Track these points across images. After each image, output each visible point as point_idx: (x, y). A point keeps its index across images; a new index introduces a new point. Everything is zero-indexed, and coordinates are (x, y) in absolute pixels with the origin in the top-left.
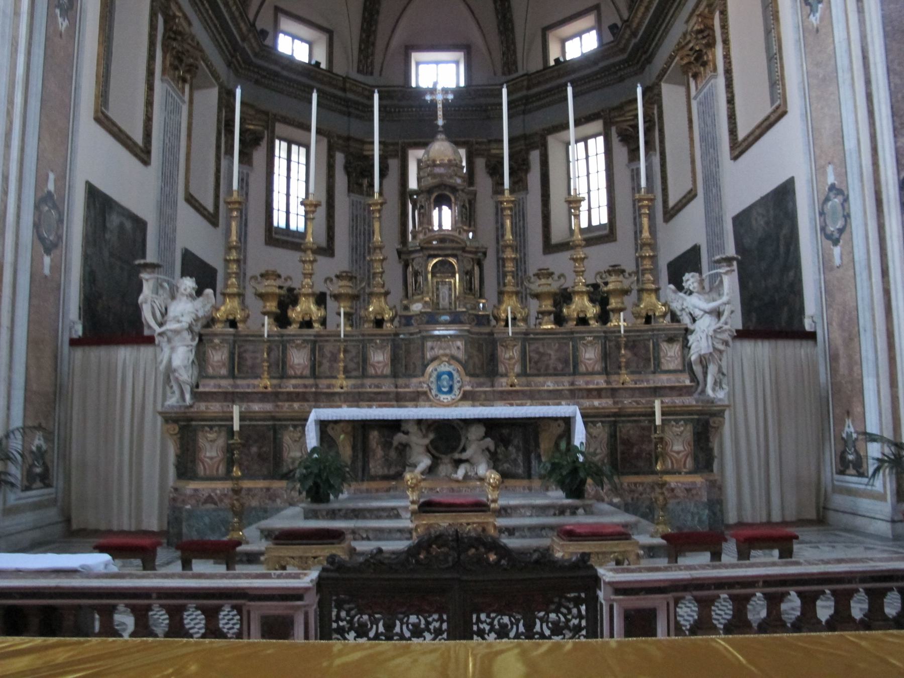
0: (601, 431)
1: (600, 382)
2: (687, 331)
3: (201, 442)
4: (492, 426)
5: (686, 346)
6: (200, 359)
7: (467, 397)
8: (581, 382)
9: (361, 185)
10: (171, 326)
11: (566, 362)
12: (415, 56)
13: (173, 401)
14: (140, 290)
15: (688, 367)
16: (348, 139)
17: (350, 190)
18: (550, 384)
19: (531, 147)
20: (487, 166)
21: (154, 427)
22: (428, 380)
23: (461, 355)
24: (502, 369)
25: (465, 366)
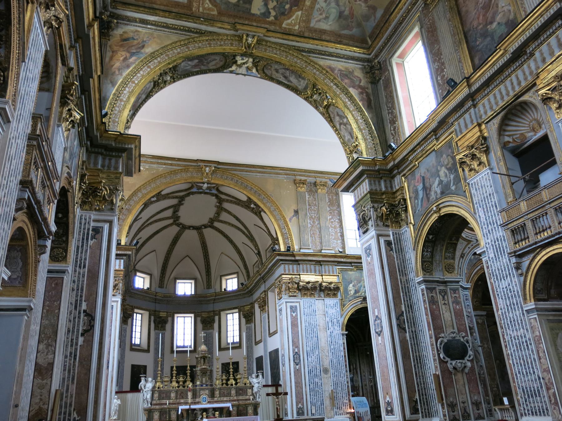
0: (235, 408)
1: (235, 398)
2: (253, 386)
3: (154, 415)
5: (252, 390)
7: (209, 402)
8: (231, 398)
9: (158, 327)
10: (147, 389)
11: (228, 394)
13: (146, 406)
14: (140, 381)
15: (253, 394)
16: (155, 311)
17: (155, 329)
18: (225, 399)
19: (215, 315)
20: (201, 320)
23: (207, 393)
24: (215, 396)
25: (208, 395)
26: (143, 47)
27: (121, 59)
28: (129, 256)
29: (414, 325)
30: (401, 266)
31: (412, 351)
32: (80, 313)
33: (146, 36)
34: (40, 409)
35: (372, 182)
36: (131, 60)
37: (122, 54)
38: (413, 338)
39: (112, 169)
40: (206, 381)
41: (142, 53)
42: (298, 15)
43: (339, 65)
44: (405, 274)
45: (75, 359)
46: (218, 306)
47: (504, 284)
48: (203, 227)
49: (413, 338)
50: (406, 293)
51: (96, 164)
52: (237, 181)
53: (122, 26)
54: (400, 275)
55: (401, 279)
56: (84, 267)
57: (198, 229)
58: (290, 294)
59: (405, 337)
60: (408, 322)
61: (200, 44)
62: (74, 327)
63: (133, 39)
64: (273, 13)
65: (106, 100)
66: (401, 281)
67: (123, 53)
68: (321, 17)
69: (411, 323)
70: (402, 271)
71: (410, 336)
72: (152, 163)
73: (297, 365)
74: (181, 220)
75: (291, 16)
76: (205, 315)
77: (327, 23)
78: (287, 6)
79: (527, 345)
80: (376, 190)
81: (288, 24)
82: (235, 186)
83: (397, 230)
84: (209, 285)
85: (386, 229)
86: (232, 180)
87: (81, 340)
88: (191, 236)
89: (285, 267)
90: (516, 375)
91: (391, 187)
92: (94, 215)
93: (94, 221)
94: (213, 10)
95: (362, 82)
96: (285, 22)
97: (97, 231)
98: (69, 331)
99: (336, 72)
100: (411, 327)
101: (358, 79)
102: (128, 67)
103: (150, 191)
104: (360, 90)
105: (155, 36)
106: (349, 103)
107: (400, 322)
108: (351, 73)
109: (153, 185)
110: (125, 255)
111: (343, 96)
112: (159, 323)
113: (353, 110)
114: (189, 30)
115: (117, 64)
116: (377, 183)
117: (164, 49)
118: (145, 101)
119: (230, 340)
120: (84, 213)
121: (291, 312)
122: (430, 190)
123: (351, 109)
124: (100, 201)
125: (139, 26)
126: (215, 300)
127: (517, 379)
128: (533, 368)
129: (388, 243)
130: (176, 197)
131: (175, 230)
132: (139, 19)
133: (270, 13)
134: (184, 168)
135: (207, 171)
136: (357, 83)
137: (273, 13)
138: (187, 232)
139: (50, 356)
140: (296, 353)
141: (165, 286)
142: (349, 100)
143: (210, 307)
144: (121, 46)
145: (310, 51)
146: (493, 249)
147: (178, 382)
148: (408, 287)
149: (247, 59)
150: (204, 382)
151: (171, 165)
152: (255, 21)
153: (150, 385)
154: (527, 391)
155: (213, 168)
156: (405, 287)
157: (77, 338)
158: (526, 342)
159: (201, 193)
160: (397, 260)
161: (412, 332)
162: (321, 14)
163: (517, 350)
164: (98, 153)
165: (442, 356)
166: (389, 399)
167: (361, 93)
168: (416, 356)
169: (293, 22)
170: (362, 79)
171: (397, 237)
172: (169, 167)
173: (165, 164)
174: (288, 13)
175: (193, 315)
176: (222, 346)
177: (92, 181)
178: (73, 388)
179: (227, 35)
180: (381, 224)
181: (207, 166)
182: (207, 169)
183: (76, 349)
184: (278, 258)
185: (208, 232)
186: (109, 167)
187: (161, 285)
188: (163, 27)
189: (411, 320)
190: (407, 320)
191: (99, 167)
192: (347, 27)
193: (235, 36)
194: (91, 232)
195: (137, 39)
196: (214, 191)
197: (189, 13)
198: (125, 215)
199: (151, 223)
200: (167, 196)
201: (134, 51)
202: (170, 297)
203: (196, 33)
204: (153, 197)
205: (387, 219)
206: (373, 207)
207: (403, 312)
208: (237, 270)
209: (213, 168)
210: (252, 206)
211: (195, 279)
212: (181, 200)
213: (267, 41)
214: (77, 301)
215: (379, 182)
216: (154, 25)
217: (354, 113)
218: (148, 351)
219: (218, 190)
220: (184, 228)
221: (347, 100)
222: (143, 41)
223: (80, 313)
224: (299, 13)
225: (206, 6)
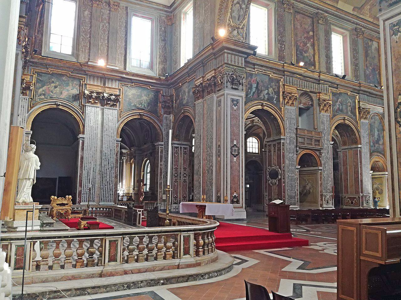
47: (291, 155)
79: (294, 180)
90: (287, 190)
122: (261, 92)
127: (287, 192)
128: (294, 188)
146: (289, 140)
154: (290, 196)
158: (294, 179)
163: (290, 181)
166: (236, 194)
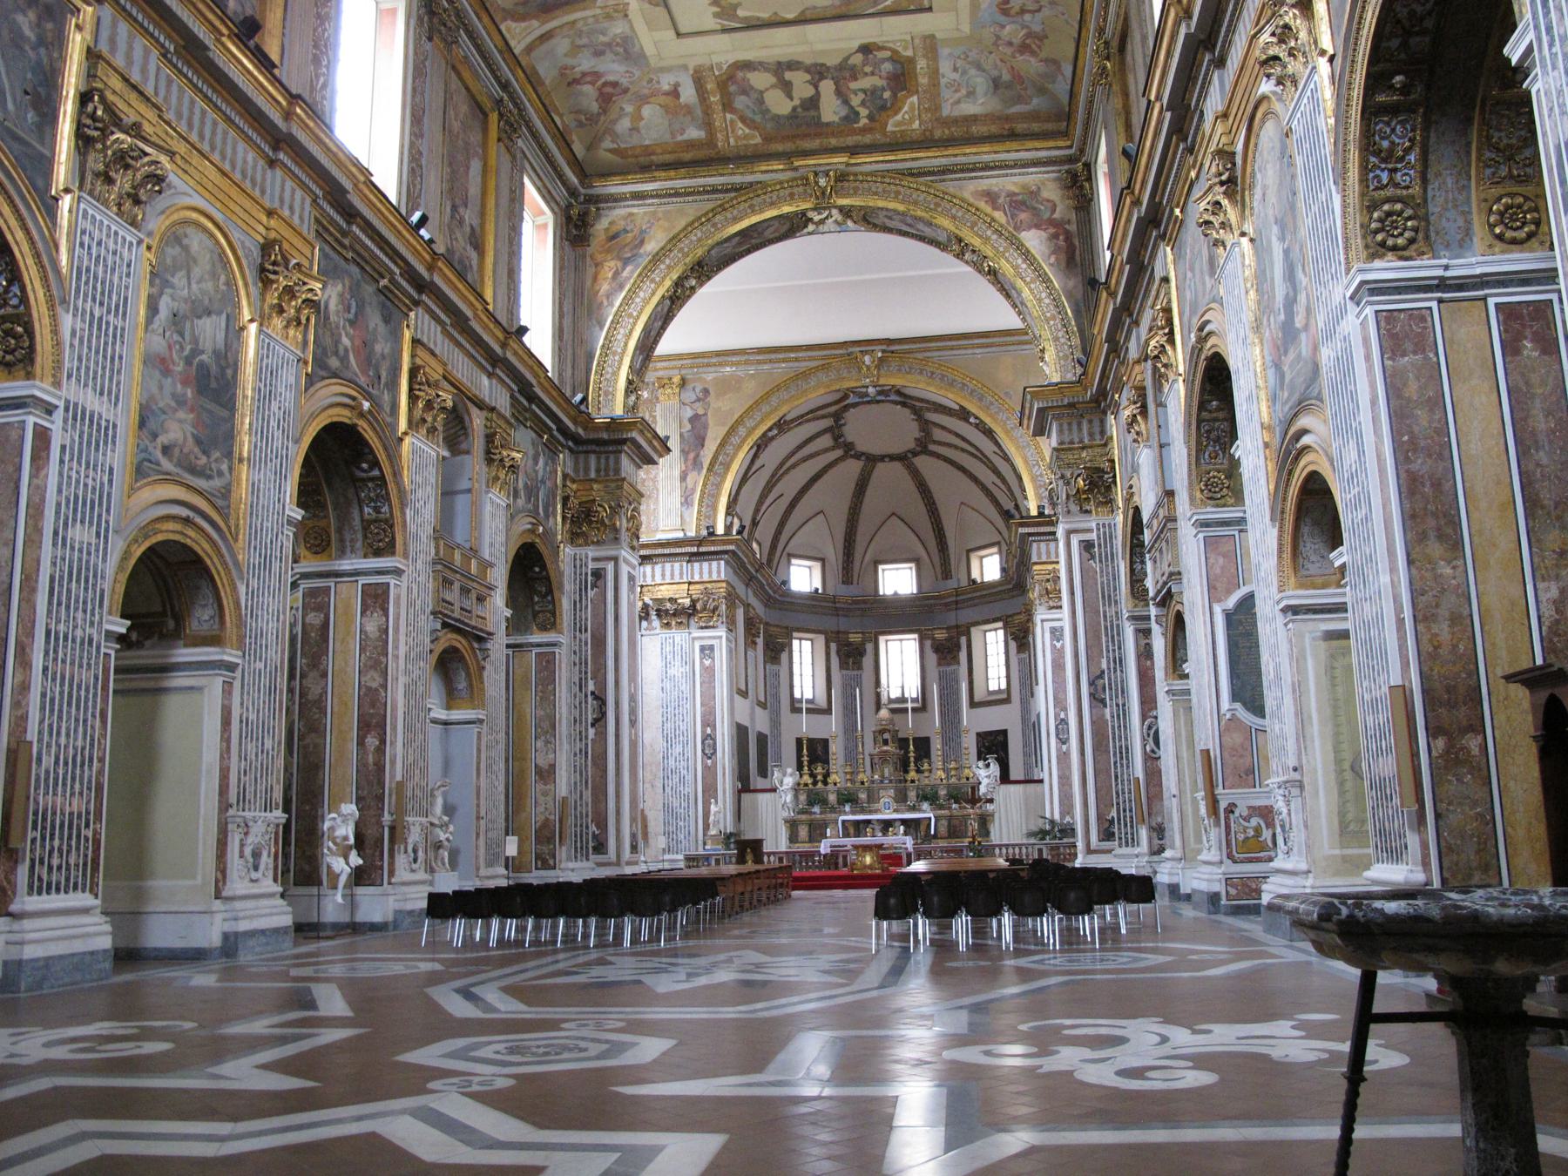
4: (904, 822)
6: (796, 797)
7: (895, 811)
10: (785, 787)
12: (881, 567)
13: (785, 814)
16: (838, 632)
17: (841, 667)
19: (960, 634)
21: (781, 823)
22: (880, 805)
26: (642, 242)
27: (610, 275)
28: (733, 552)
29: (1123, 692)
30: (1109, 586)
31: (1114, 738)
32: (586, 696)
33: (646, 219)
34: (547, 819)
35: (1065, 426)
36: (625, 274)
37: (610, 266)
38: (1118, 716)
39: (611, 473)
40: (890, 774)
41: (641, 256)
42: (912, 104)
43: (1009, 183)
44: (1116, 602)
45: (586, 757)
46: (965, 615)
48: (910, 455)
49: (1118, 716)
50: (1113, 637)
51: (587, 470)
52: (933, 373)
53: (606, 212)
54: (1104, 605)
55: (1105, 612)
56: (586, 630)
57: (901, 458)
58: (1051, 603)
59: (1103, 715)
60: (1111, 689)
61: (735, 212)
62: (581, 715)
63: (626, 231)
64: (864, 112)
65: (590, 357)
66: (1105, 616)
67: (612, 264)
68: (957, 95)
69: (1117, 690)
70: (1109, 596)
71: (1112, 713)
72: (759, 362)
73: (1064, 743)
74: (862, 446)
75: (900, 109)
76: (941, 635)
77: (974, 103)
78: (887, 95)
80: (1072, 442)
81: (899, 124)
82: (928, 384)
83: (1106, 520)
84: (947, 574)
85: (1086, 517)
86: (921, 373)
87: (591, 732)
88: (889, 475)
89: (1039, 548)
91: (1103, 432)
92: (591, 552)
93: (595, 560)
94: (753, 137)
95: (1058, 209)
96: (891, 122)
97: (598, 575)
98: (575, 721)
99: (1001, 201)
100: (1117, 697)
101: (1049, 205)
102: (621, 287)
103: (762, 421)
104: (1052, 230)
105: (660, 215)
106: (1024, 266)
107: (1096, 690)
108: (1034, 194)
109: (766, 408)
110: (726, 552)
111: (1012, 253)
112: (848, 656)
113: (1031, 282)
114: (714, 190)
115: (605, 287)
116: (1075, 427)
117: (674, 240)
118: (663, 328)
119: (993, 686)
120: (578, 551)
121: (1052, 640)
123: (1028, 279)
124: (598, 529)
125: (633, 206)
126: (957, 602)
129: (1087, 546)
130: (823, 417)
131: (853, 467)
132: (631, 193)
133: (857, 114)
134: (821, 362)
135: (867, 363)
136: (1046, 216)
137: (864, 112)
138: (880, 466)
139: (552, 756)
140: (1062, 720)
141: (855, 582)
142: (1024, 261)
143: (952, 618)
144: (608, 251)
145: (944, 171)
147: (812, 775)
148: (1118, 626)
149: (827, 213)
150: (887, 775)
151: (797, 360)
152: (833, 135)
153: (789, 781)
155: (880, 355)
156: (1112, 626)
157: (587, 730)
159: (869, 402)
160: (1102, 576)
161: (1118, 705)
162: (956, 91)
164: (587, 452)
165: (1148, 748)
167: (1055, 236)
168: (1121, 747)
169: (907, 117)
170: (1058, 203)
171: (1105, 533)
172: (791, 364)
173: (784, 361)
174: (892, 105)
175: (916, 636)
176: (977, 698)
177: (584, 499)
178: (588, 795)
179: (781, 183)
180: (1074, 508)
181: (866, 352)
182: (867, 359)
183: (587, 745)
184: (1022, 530)
185: (922, 462)
186: (607, 470)
187: (847, 576)
188: (671, 196)
189: (1116, 685)
190: (1110, 684)
191: (593, 475)
192: (1019, 99)
193: (796, 179)
194: (590, 578)
195: (632, 231)
196: (893, 397)
197: (711, 153)
198: (719, 475)
199: (794, 466)
200: (801, 419)
201: (629, 255)
202: (865, 602)
203: (727, 191)
204: (770, 429)
205: (1088, 499)
206: (1063, 477)
207: (1103, 672)
208: (997, 538)
209: (880, 355)
210: (972, 420)
211: (917, 561)
212: (837, 416)
213: (856, 175)
214: (581, 679)
215: (1079, 424)
216: (657, 196)
217: (1033, 286)
218: (828, 711)
219: (899, 393)
220: (872, 460)
221: (1020, 261)
222: (642, 232)
223: (586, 696)
224: (915, 99)
225: (740, 132)
